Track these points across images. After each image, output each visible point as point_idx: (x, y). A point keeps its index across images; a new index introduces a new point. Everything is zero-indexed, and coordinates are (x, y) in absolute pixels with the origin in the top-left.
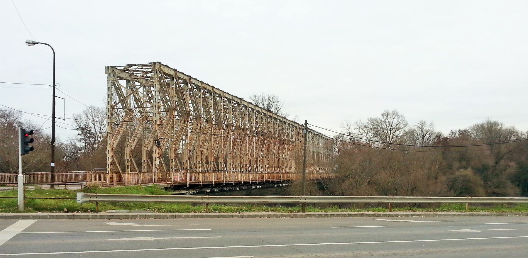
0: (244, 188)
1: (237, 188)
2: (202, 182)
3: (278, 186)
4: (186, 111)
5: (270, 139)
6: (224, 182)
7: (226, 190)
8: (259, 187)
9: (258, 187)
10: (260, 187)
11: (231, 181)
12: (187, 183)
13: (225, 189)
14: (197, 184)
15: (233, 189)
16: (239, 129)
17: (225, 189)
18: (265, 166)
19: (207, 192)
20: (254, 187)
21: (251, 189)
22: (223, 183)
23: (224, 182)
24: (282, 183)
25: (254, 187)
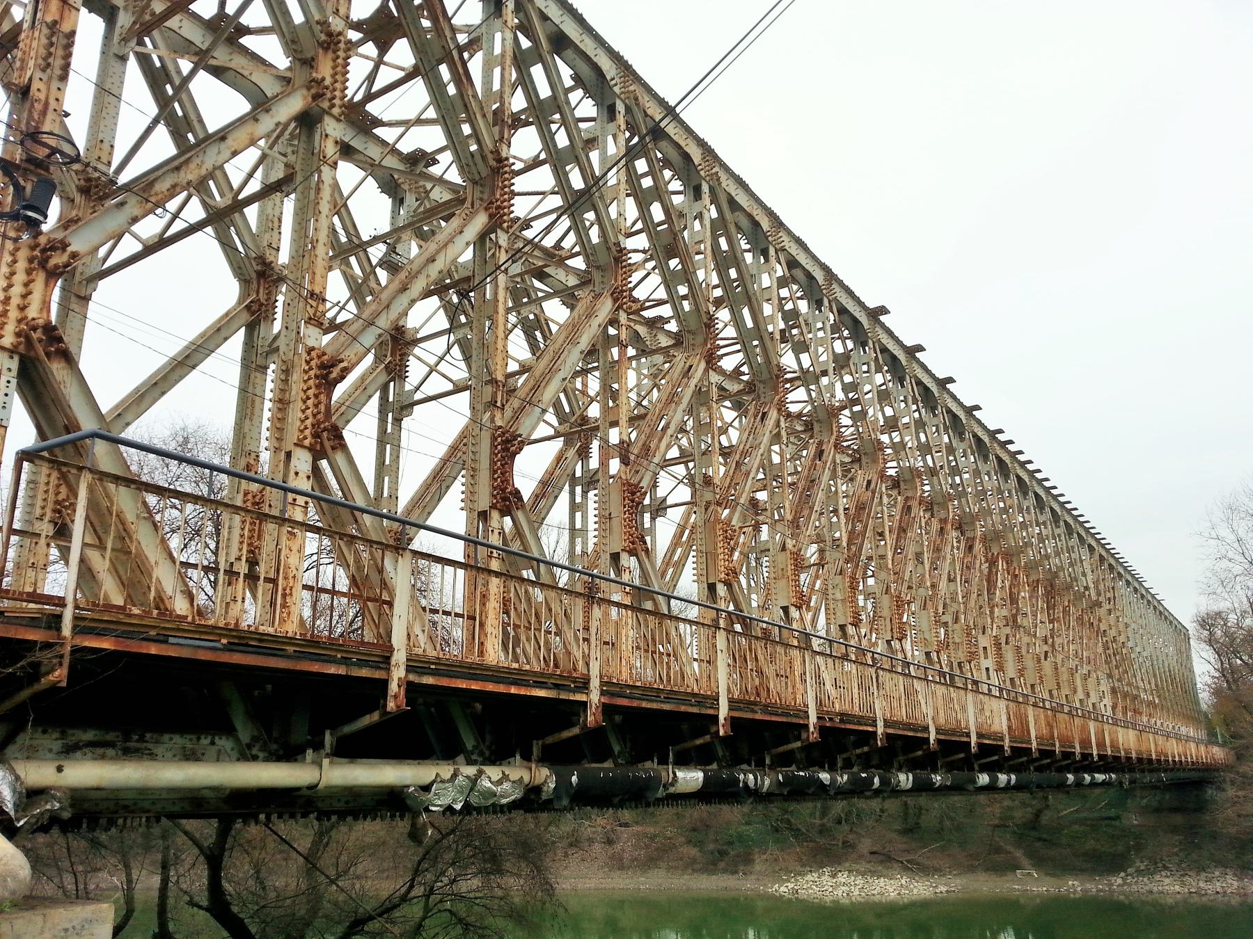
0: (937, 779)
1: (902, 777)
2: (595, 683)
3: (1079, 784)
4: (484, 158)
5: (1015, 564)
6: (813, 719)
7: (833, 781)
8: (1009, 781)
9: (1002, 778)
10: (1013, 782)
11: (860, 720)
12: (387, 660)
13: (825, 777)
14: (542, 693)
15: (876, 780)
16: (875, 461)
17: (825, 777)
18: (1012, 679)
19: (681, 788)
20: (984, 779)
21: (971, 787)
22: (806, 726)
23: (813, 719)
24: (1092, 769)
25: (984, 779)
